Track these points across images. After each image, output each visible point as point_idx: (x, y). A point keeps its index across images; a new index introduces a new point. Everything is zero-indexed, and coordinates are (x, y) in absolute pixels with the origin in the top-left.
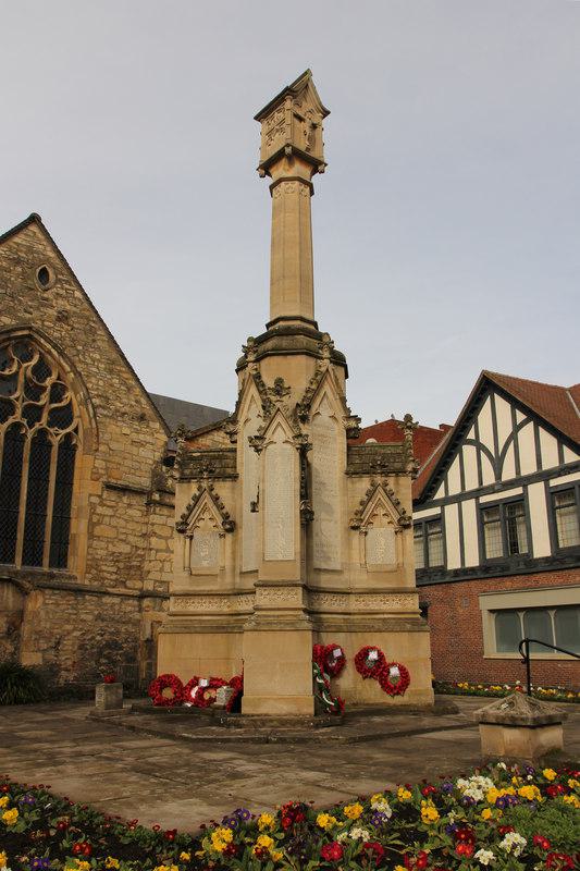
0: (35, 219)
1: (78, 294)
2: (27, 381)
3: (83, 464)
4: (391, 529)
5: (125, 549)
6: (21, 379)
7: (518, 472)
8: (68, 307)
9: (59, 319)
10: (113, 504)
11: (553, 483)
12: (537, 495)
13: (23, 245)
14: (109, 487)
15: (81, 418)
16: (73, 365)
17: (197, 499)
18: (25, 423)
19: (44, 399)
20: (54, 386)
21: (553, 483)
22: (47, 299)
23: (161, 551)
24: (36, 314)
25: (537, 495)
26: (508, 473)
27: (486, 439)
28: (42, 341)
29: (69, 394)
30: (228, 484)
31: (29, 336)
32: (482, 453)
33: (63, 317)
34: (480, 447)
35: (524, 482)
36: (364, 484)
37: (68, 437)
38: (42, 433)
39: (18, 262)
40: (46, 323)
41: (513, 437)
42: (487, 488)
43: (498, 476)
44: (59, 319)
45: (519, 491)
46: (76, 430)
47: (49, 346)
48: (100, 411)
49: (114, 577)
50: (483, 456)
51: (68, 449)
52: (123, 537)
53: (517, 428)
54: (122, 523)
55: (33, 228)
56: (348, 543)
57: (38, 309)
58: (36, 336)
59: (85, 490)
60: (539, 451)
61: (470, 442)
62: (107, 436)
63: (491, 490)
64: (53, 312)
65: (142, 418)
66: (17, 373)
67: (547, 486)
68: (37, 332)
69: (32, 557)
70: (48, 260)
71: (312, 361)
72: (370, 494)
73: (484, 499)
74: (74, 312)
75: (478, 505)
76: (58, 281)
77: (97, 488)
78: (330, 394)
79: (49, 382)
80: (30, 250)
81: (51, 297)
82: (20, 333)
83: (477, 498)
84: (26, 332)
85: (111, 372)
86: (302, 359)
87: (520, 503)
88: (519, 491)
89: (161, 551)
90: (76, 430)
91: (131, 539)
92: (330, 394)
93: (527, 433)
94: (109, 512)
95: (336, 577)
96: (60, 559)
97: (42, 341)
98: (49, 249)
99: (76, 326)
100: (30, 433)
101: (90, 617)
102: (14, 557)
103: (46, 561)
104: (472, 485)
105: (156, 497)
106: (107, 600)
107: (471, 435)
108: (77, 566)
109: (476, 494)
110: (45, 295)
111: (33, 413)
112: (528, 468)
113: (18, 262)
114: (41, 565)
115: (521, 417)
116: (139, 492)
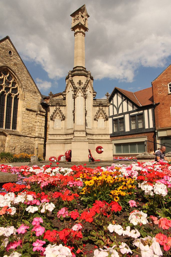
0: (7, 38)
1: (19, 59)
2: (6, 81)
3: (20, 103)
4: (104, 120)
5: (31, 125)
6: (4, 80)
7: (123, 111)
8: (17, 62)
9: (14, 65)
10: (28, 114)
11: (131, 114)
12: (127, 117)
13: (5, 44)
14: (27, 110)
15: (20, 91)
16: (18, 77)
17: (55, 111)
18: (6, 91)
19: (10, 86)
20: (13, 83)
21: (131, 114)
22: (11, 59)
23: (40, 126)
25: (127, 117)
26: (120, 112)
27: (115, 103)
29: (17, 85)
30: (64, 107)
32: (114, 108)
33: (15, 64)
34: (114, 105)
35: (124, 114)
36: (97, 108)
37: (17, 96)
38: (10, 95)
39: (3, 48)
40: (11, 66)
41: (122, 103)
42: (115, 115)
43: (118, 112)
44: (14, 65)
45: (123, 116)
46: (19, 94)
48: (25, 90)
49: (28, 132)
50: (114, 108)
51: (16, 99)
52: (30, 122)
53: (123, 101)
54: (30, 118)
55: (8, 40)
56: (93, 123)
57: (9, 61)
60: (126, 107)
61: (111, 104)
62: (26, 96)
63: (116, 116)
64: (13, 63)
65: (35, 92)
66: (3, 78)
67: (129, 115)
69: (8, 127)
71: (86, 78)
72: (99, 111)
73: (114, 118)
74: (18, 64)
75: (113, 119)
77: (24, 109)
78: (90, 86)
79: (11, 81)
80: (7, 46)
81: (12, 59)
82: (4, 68)
83: (112, 117)
84: (6, 68)
85: (28, 80)
86: (84, 77)
87: (123, 119)
88: (123, 116)
89: (40, 126)
90: (19, 94)
91: (33, 123)
92: (90, 86)
93: (125, 103)
94: (27, 116)
95: (90, 130)
96: (14, 127)
98: (11, 46)
99: (19, 67)
100: (7, 94)
101: (22, 142)
102: (3, 126)
103: (11, 128)
104: (111, 114)
105: (39, 112)
106: (26, 138)
107: (112, 102)
108: (19, 129)
109: (112, 117)
110: (11, 58)
111: (7, 89)
112: (125, 111)
113: (3, 48)
114: (10, 129)
115: (124, 98)
116: (35, 111)
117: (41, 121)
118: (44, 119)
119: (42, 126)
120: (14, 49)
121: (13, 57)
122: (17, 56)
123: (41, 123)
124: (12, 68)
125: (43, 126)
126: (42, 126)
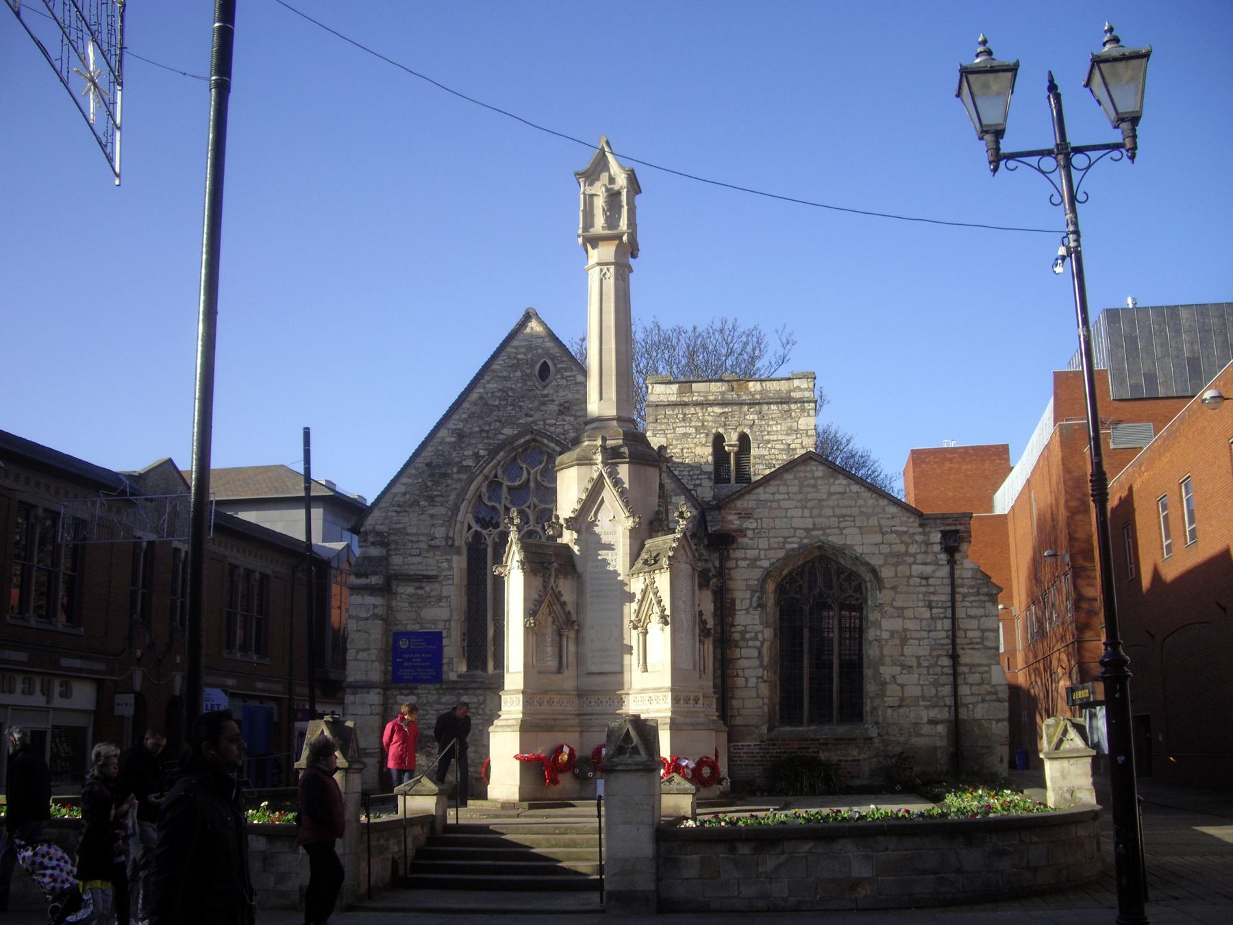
6: (532, 484)
8: (570, 396)
9: (561, 413)
22: (546, 396)
24: (538, 416)
28: (545, 441)
31: (534, 440)
44: (561, 413)
47: (552, 445)
57: (538, 409)
58: (538, 438)
64: (553, 407)
66: (528, 480)
68: (539, 433)
70: (547, 353)
76: (558, 371)
81: (551, 392)
82: (522, 440)
84: (528, 437)
97: (545, 441)
110: (546, 392)
120: (556, 350)
121: (554, 383)
122: (571, 370)
124: (553, 429)
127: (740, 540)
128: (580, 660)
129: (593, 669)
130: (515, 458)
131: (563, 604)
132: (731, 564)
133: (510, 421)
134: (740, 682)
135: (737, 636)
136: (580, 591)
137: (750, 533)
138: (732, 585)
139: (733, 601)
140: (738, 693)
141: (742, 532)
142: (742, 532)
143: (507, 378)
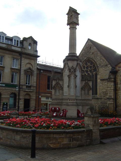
3: (98, 76)
5: (105, 90)
10: (102, 83)
23: (110, 90)
44: (92, 54)
49: (103, 96)
54: (104, 86)
59: (99, 81)
64: (91, 53)
89: (110, 90)
101: (100, 103)
106: (102, 100)
117: (111, 86)
118: (113, 84)
119: (111, 90)
123: (111, 87)
125: (112, 90)
126: (111, 90)
127: (119, 72)
128: (63, 93)
129: (64, 95)
130: (87, 62)
131: (60, 85)
132: (117, 76)
133: (86, 57)
134: (119, 97)
135: (118, 89)
136: (63, 83)
137: (120, 70)
138: (117, 80)
139: (118, 82)
140: (119, 99)
141: (119, 70)
142: (119, 70)
143: (86, 50)
